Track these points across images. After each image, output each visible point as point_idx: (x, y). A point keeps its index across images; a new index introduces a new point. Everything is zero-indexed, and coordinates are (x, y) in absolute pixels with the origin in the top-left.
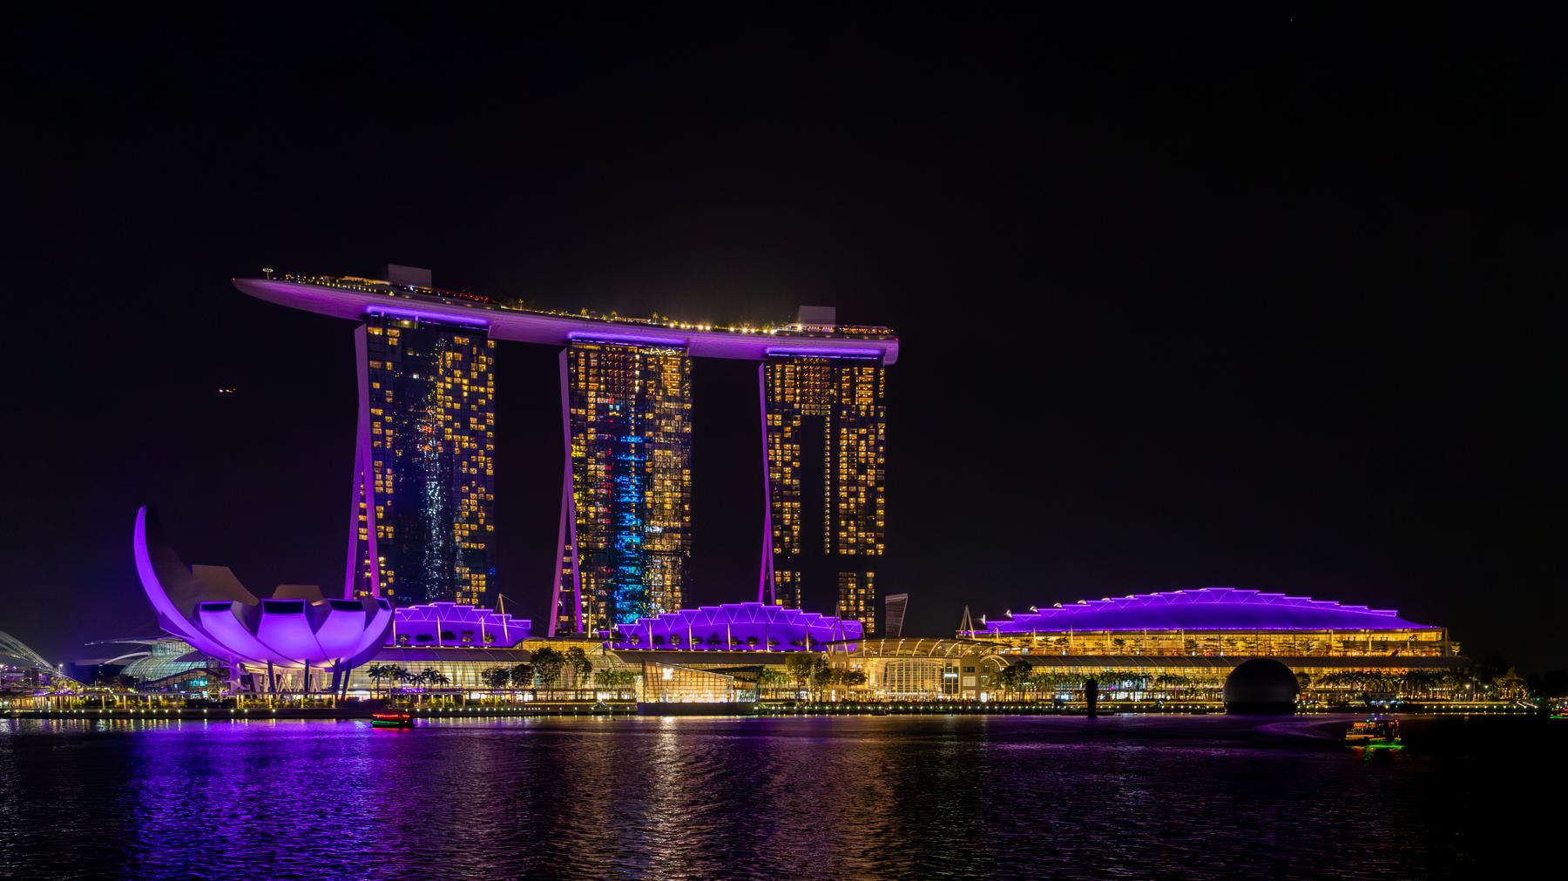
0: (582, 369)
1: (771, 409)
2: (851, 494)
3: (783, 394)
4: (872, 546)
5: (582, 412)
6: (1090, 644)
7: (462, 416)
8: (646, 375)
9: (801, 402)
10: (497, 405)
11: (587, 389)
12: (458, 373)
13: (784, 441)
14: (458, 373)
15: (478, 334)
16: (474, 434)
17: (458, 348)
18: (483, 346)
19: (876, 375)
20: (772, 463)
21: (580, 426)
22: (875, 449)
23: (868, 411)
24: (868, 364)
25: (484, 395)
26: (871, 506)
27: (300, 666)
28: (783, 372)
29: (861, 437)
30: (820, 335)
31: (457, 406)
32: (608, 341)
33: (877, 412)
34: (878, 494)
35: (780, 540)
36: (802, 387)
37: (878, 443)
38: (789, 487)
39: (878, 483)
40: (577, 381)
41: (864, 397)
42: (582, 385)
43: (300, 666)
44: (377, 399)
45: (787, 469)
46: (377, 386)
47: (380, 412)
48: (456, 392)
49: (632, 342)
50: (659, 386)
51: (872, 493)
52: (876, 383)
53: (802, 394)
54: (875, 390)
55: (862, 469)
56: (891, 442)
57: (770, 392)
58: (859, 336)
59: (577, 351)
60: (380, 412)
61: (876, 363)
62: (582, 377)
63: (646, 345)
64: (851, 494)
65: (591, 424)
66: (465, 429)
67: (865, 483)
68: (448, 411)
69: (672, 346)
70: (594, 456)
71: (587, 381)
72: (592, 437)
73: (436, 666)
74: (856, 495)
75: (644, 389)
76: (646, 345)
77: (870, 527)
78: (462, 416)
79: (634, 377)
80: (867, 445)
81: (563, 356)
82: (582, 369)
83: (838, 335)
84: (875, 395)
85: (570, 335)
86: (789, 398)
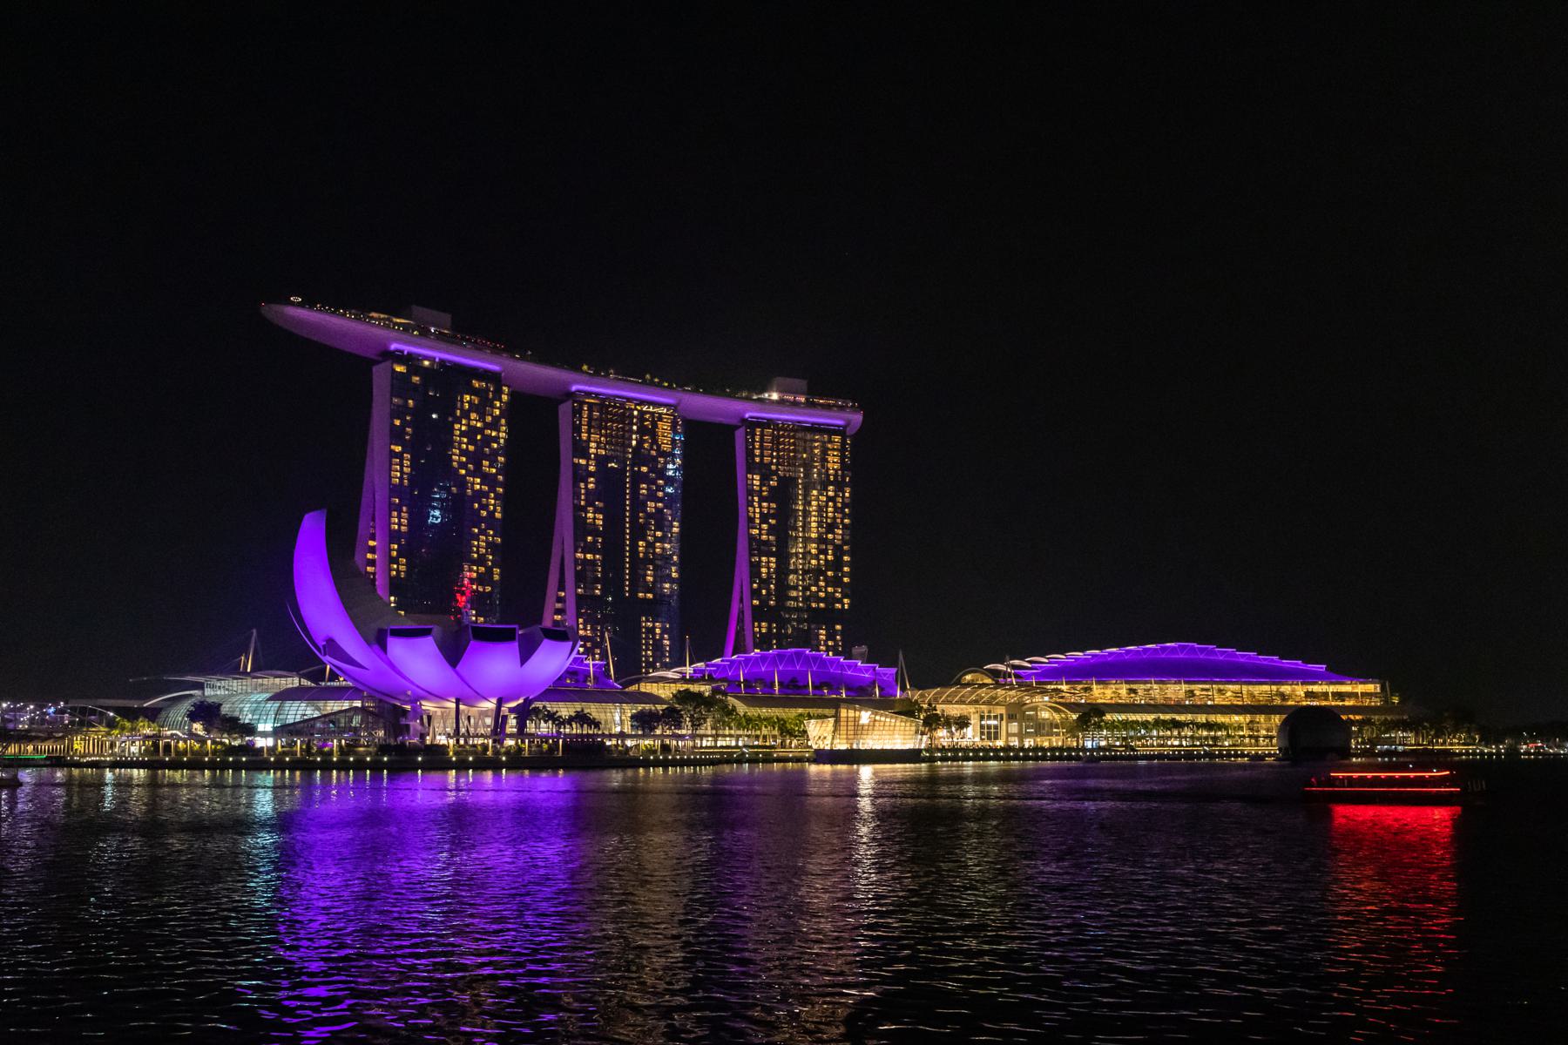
0: (584, 421)
1: (751, 468)
2: (821, 552)
3: (762, 456)
4: (840, 601)
5: (583, 462)
6: (1109, 692)
7: (476, 458)
8: (642, 431)
9: (778, 464)
10: (508, 449)
11: (589, 440)
12: (473, 416)
13: (762, 499)
14: (473, 416)
15: (494, 378)
16: (486, 479)
17: (473, 392)
18: (498, 393)
19: (843, 443)
20: (751, 520)
21: (580, 475)
22: (841, 511)
23: (836, 475)
24: (836, 433)
25: (496, 439)
26: (837, 565)
27: (490, 705)
28: (762, 436)
29: (830, 499)
30: (795, 404)
31: (471, 448)
32: (608, 397)
33: (843, 477)
34: (844, 553)
35: (756, 594)
36: (778, 451)
37: (845, 505)
38: (767, 543)
39: (845, 542)
40: (580, 433)
41: (833, 463)
42: (585, 436)
43: (490, 705)
44: (396, 435)
45: (765, 526)
46: (397, 422)
47: (398, 449)
48: (471, 433)
49: (629, 400)
50: (654, 441)
51: (838, 551)
52: (842, 450)
53: (778, 457)
54: (842, 457)
55: (831, 528)
56: (854, 503)
57: (750, 454)
58: (829, 407)
59: (582, 403)
60: (398, 449)
61: (841, 432)
62: (584, 428)
63: (642, 402)
64: (821, 552)
65: (591, 474)
66: (478, 472)
67: (832, 542)
68: (463, 453)
69: (665, 405)
70: (592, 505)
71: (589, 432)
72: (591, 486)
73: (593, 710)
74: (825, 552)
75: (640, 442)
76: (642, 402)
77: (836, 582)
78: (476, 458)
79: (632, 432)
80: (835, 507)
81: (565, 409)
82: (584, 421)
83: (810, 404)
84: (842, 462)
85: (574, 388)
86: (767, 460)
